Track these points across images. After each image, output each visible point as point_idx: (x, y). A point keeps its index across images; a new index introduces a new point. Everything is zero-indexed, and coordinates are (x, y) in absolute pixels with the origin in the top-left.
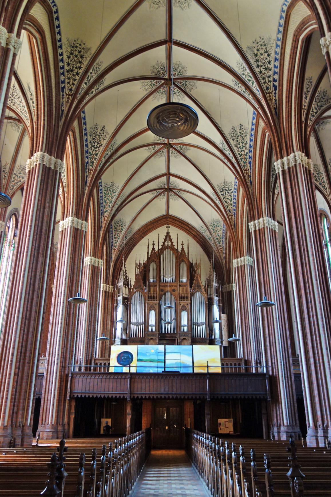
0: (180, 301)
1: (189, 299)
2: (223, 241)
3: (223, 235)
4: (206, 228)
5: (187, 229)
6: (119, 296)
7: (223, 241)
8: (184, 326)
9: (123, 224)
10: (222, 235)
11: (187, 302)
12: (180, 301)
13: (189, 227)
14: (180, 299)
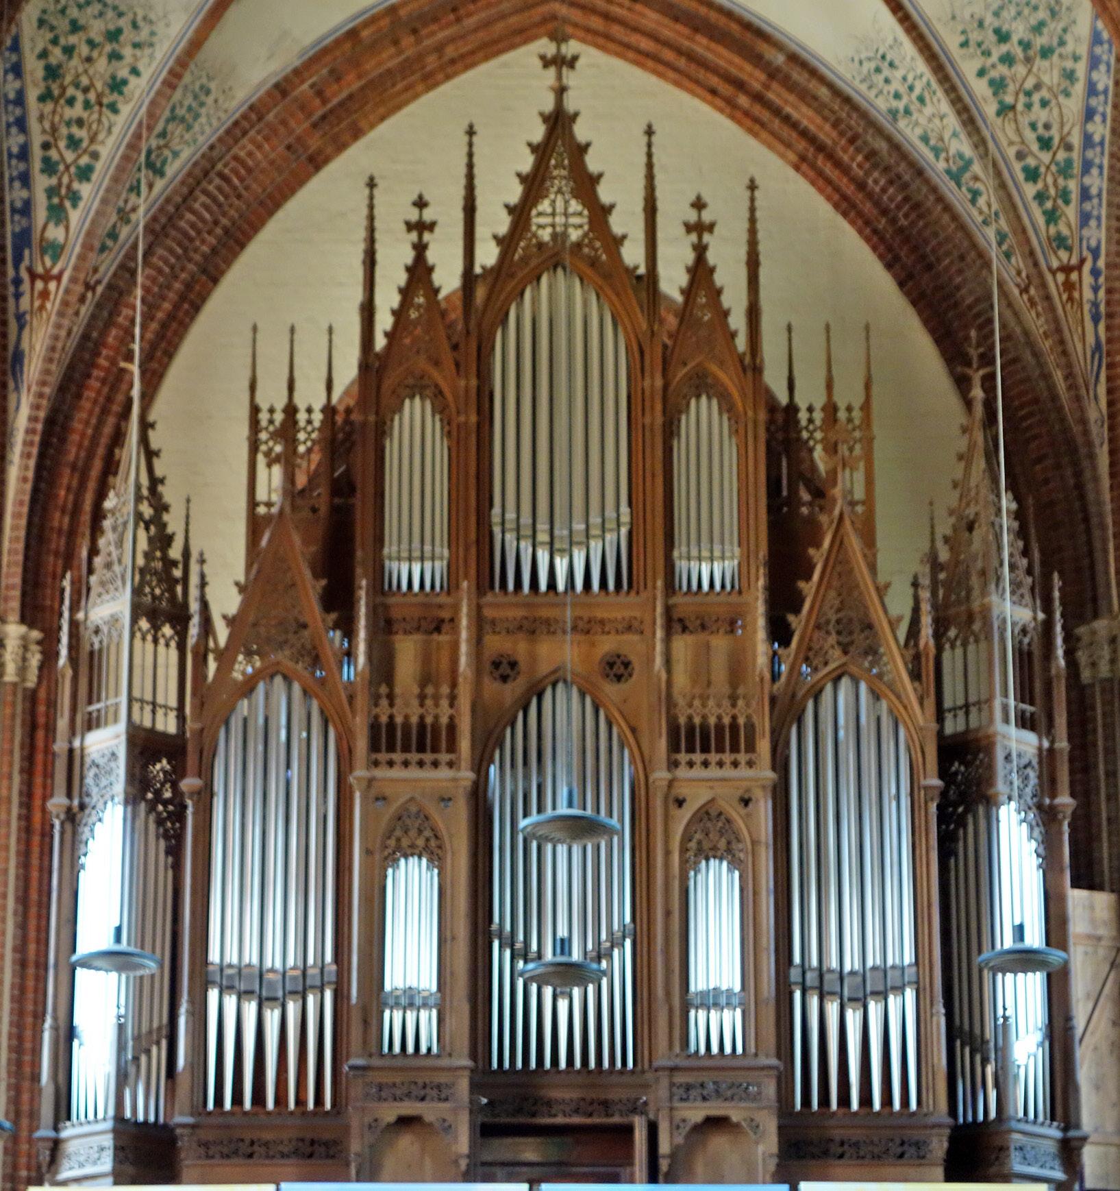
0: (673, 764)
1: (764, 746)
2: (1085, 194)
3: (1088, 140)
4: (921, 66)
5: (740, 85)
6: (92, 723)
7: (1085, 194)
8: (713, 1000)
9: (128, 35)
10: (1076, 139)
11: (744, 772)
12: (673, 764)
13: (757, 60)
14: (674, 747)
